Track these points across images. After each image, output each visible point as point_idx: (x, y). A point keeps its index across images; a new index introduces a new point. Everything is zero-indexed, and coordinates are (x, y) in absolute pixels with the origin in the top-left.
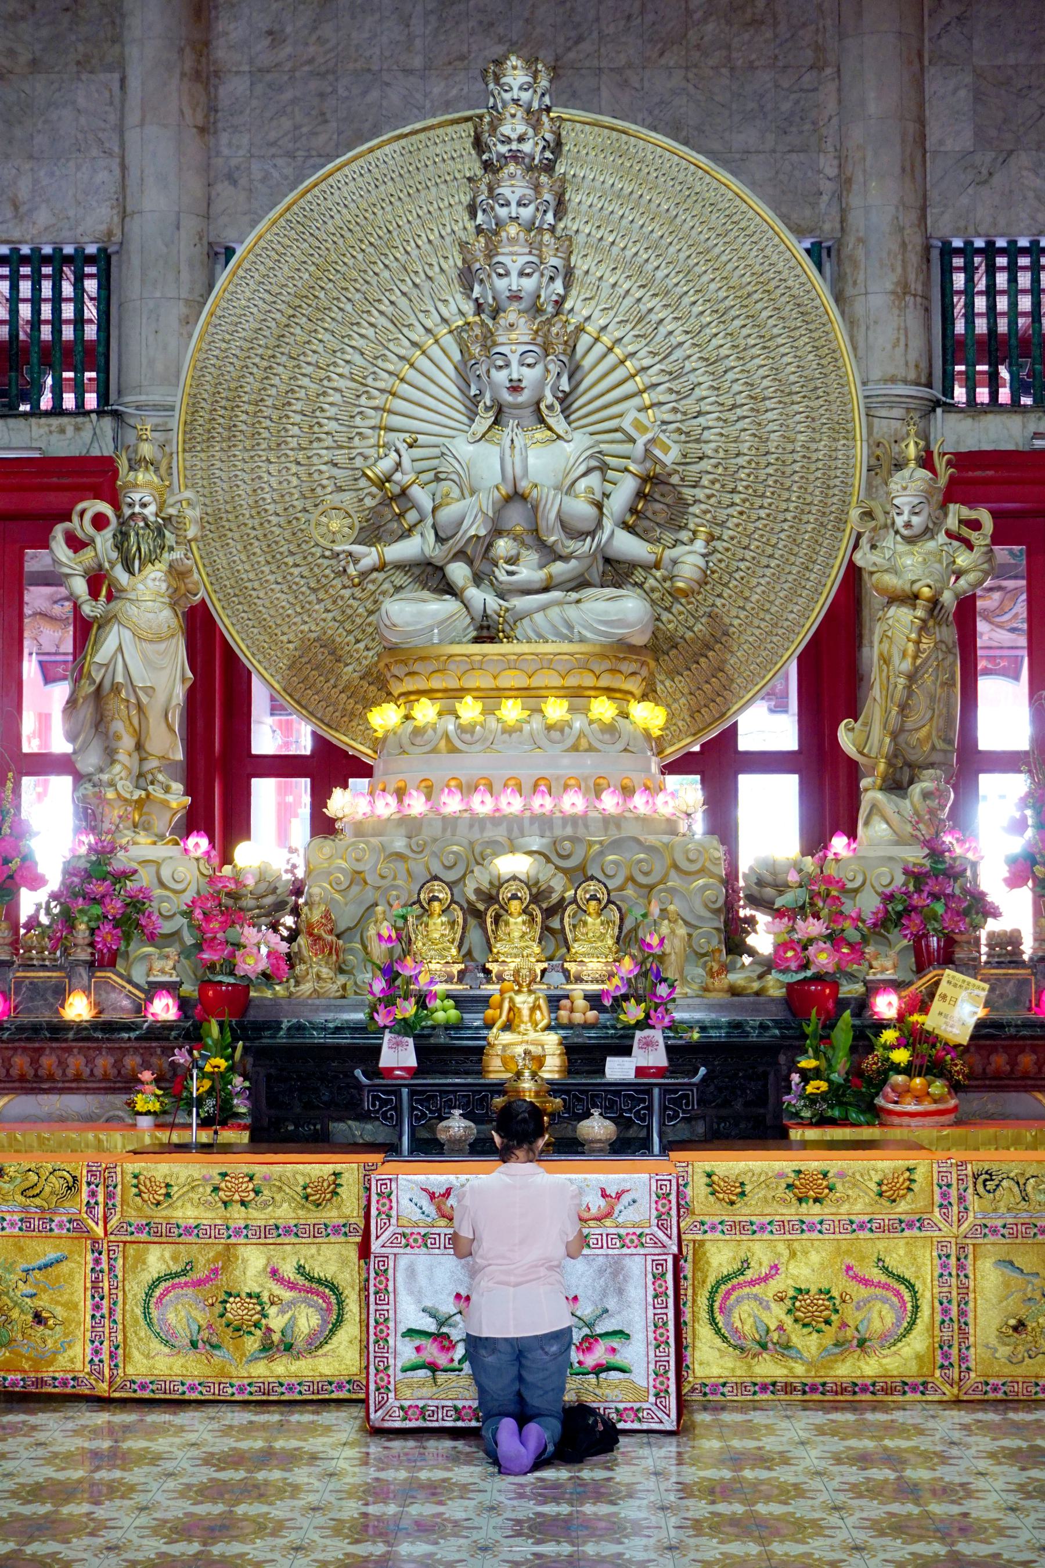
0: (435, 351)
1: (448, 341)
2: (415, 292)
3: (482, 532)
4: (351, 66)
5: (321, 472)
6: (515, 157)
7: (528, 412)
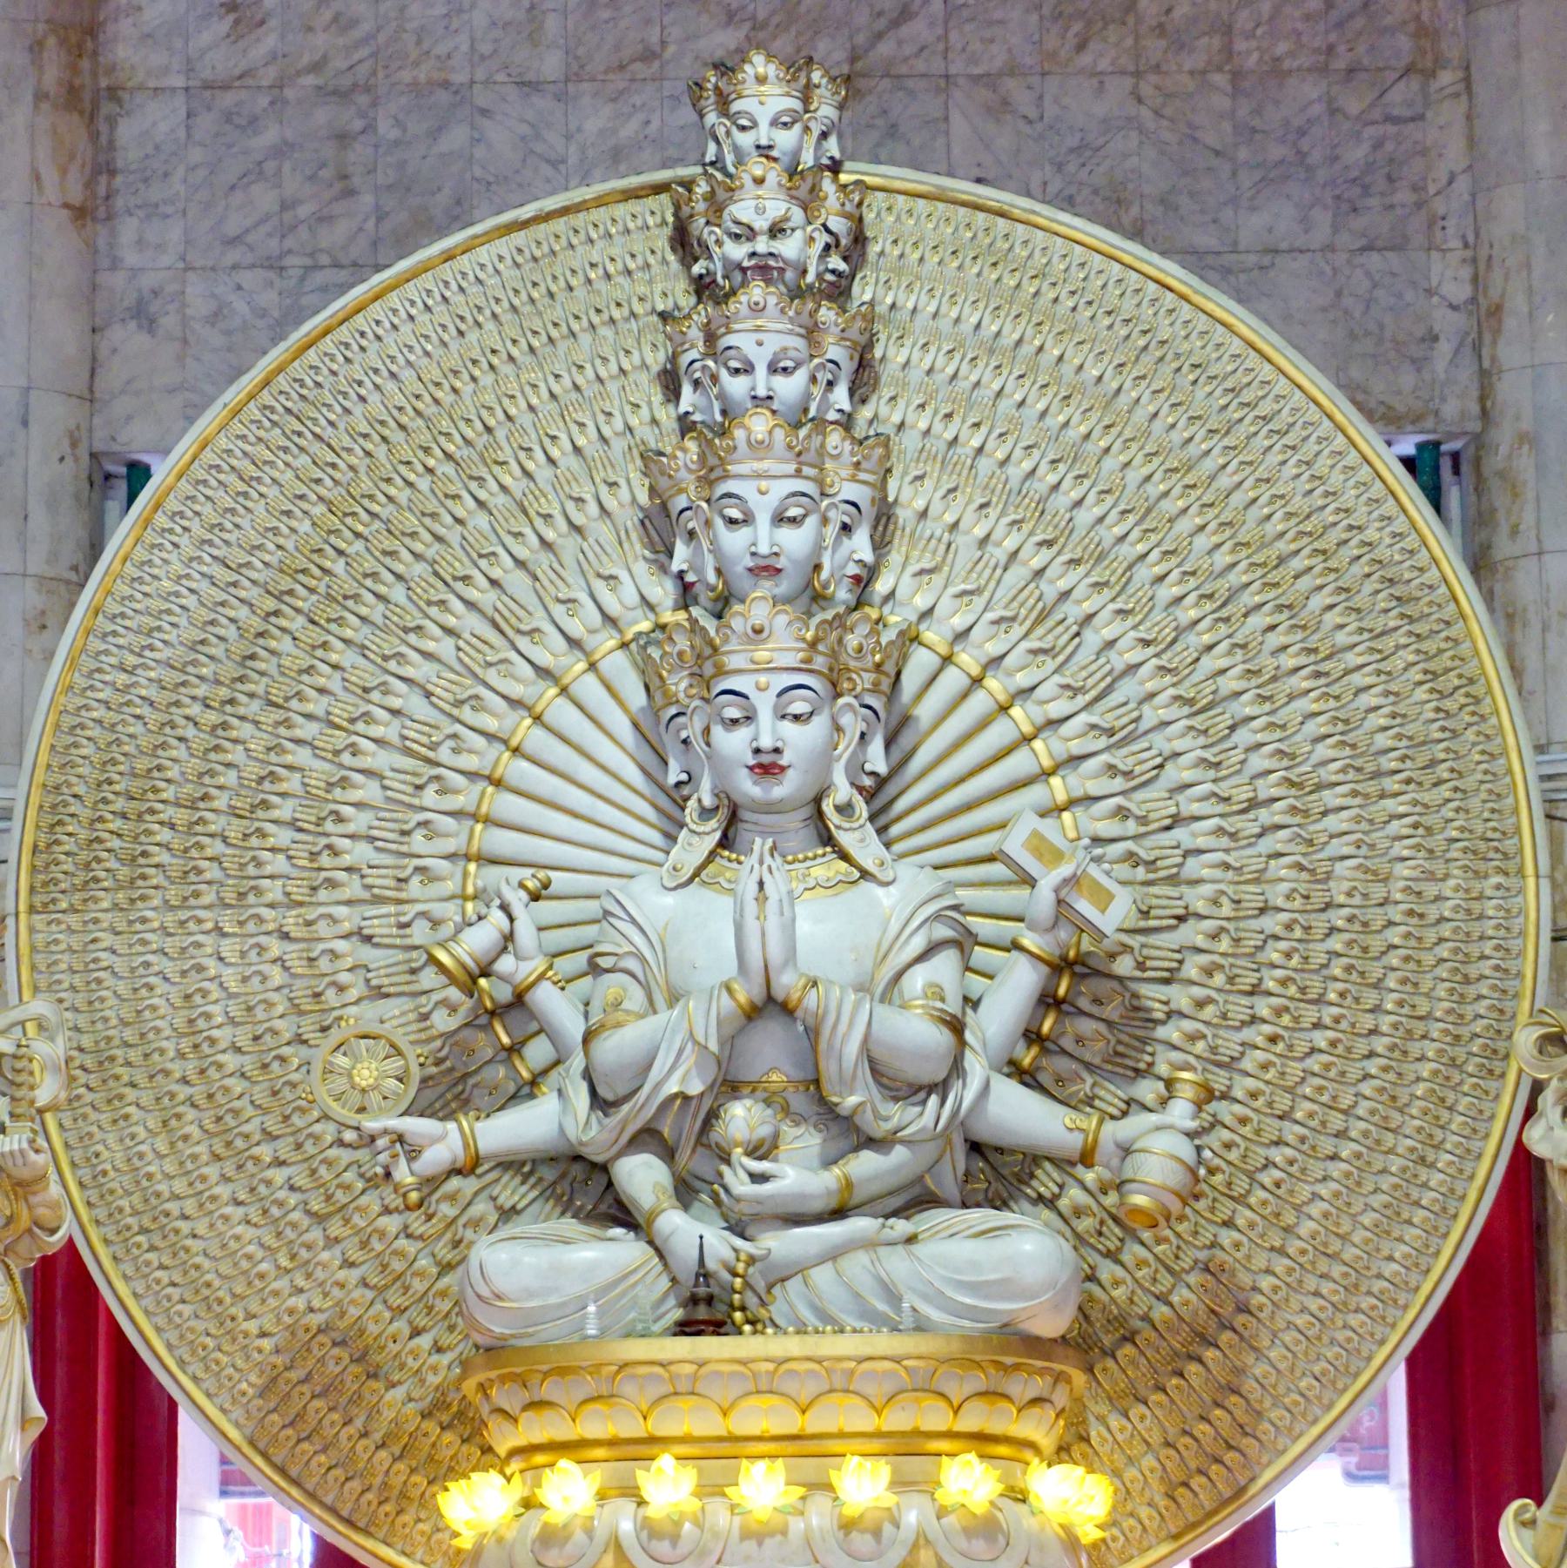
0: (589, 689)
1: (619, 667)
2: (545, 558)
3: (695, 1088)
4: (406, 76)
5: (334, 955)
6: (764, 269)
7: (794, 821)
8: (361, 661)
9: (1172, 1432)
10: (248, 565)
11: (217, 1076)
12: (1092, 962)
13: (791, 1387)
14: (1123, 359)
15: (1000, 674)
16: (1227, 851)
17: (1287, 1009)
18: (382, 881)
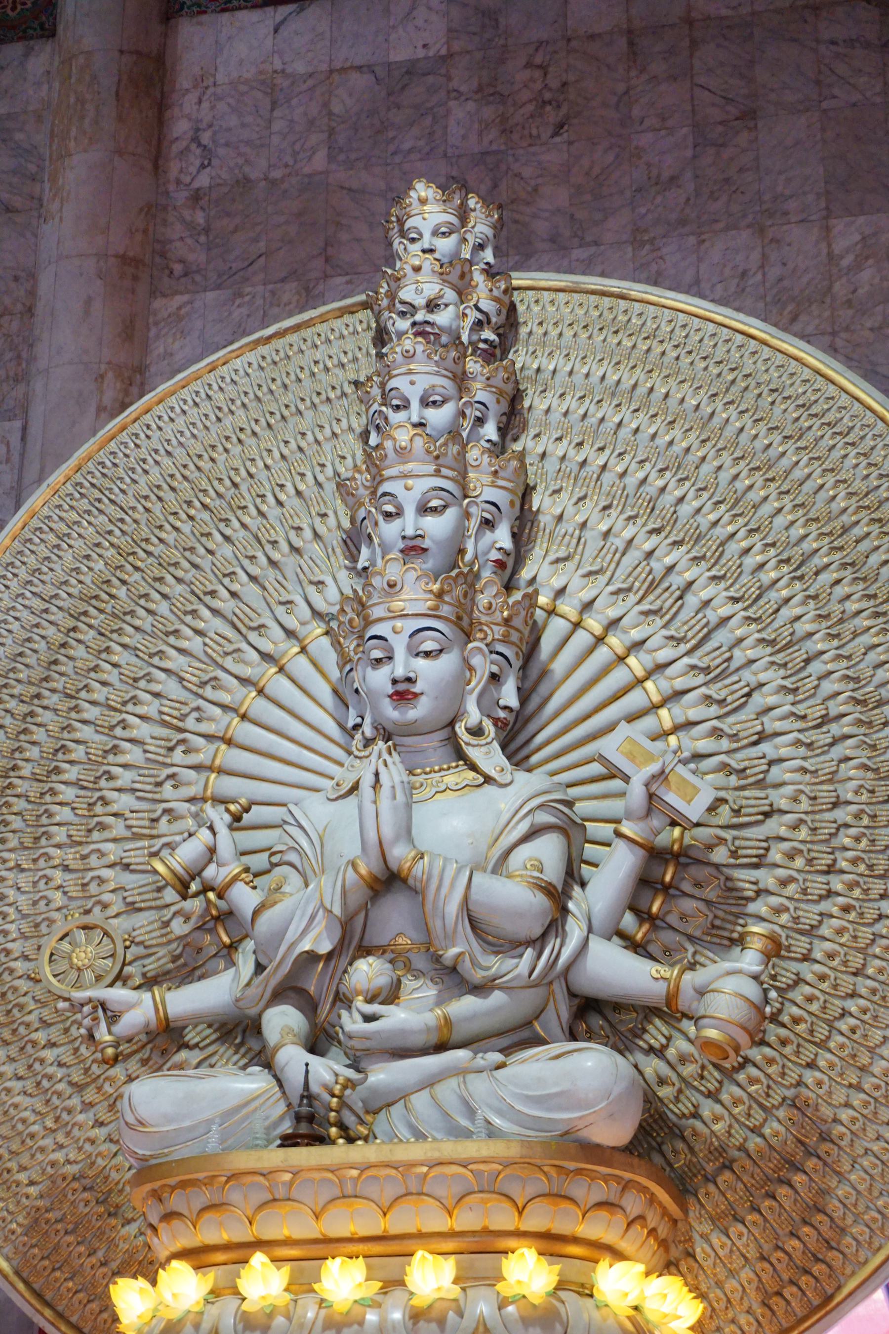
0: (301, 666)
1: (322, 647)
2: (271, 573)
5: (101, 881)
7: (433, 742)
8: (134, 660)
9: (767, 1247)
10: (56, 596)
11: (9, 978)
12: (693, 853)
13: (372, 1190)
14: (715, 391)
15: (618, 633)
16: (804, 758)
17: (857, 884)
18: (139, 822)
